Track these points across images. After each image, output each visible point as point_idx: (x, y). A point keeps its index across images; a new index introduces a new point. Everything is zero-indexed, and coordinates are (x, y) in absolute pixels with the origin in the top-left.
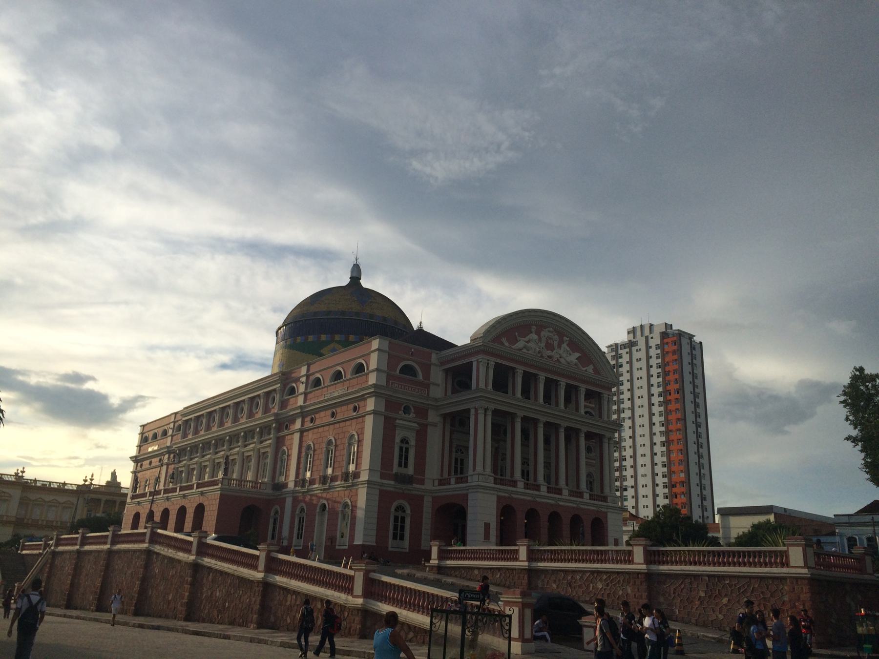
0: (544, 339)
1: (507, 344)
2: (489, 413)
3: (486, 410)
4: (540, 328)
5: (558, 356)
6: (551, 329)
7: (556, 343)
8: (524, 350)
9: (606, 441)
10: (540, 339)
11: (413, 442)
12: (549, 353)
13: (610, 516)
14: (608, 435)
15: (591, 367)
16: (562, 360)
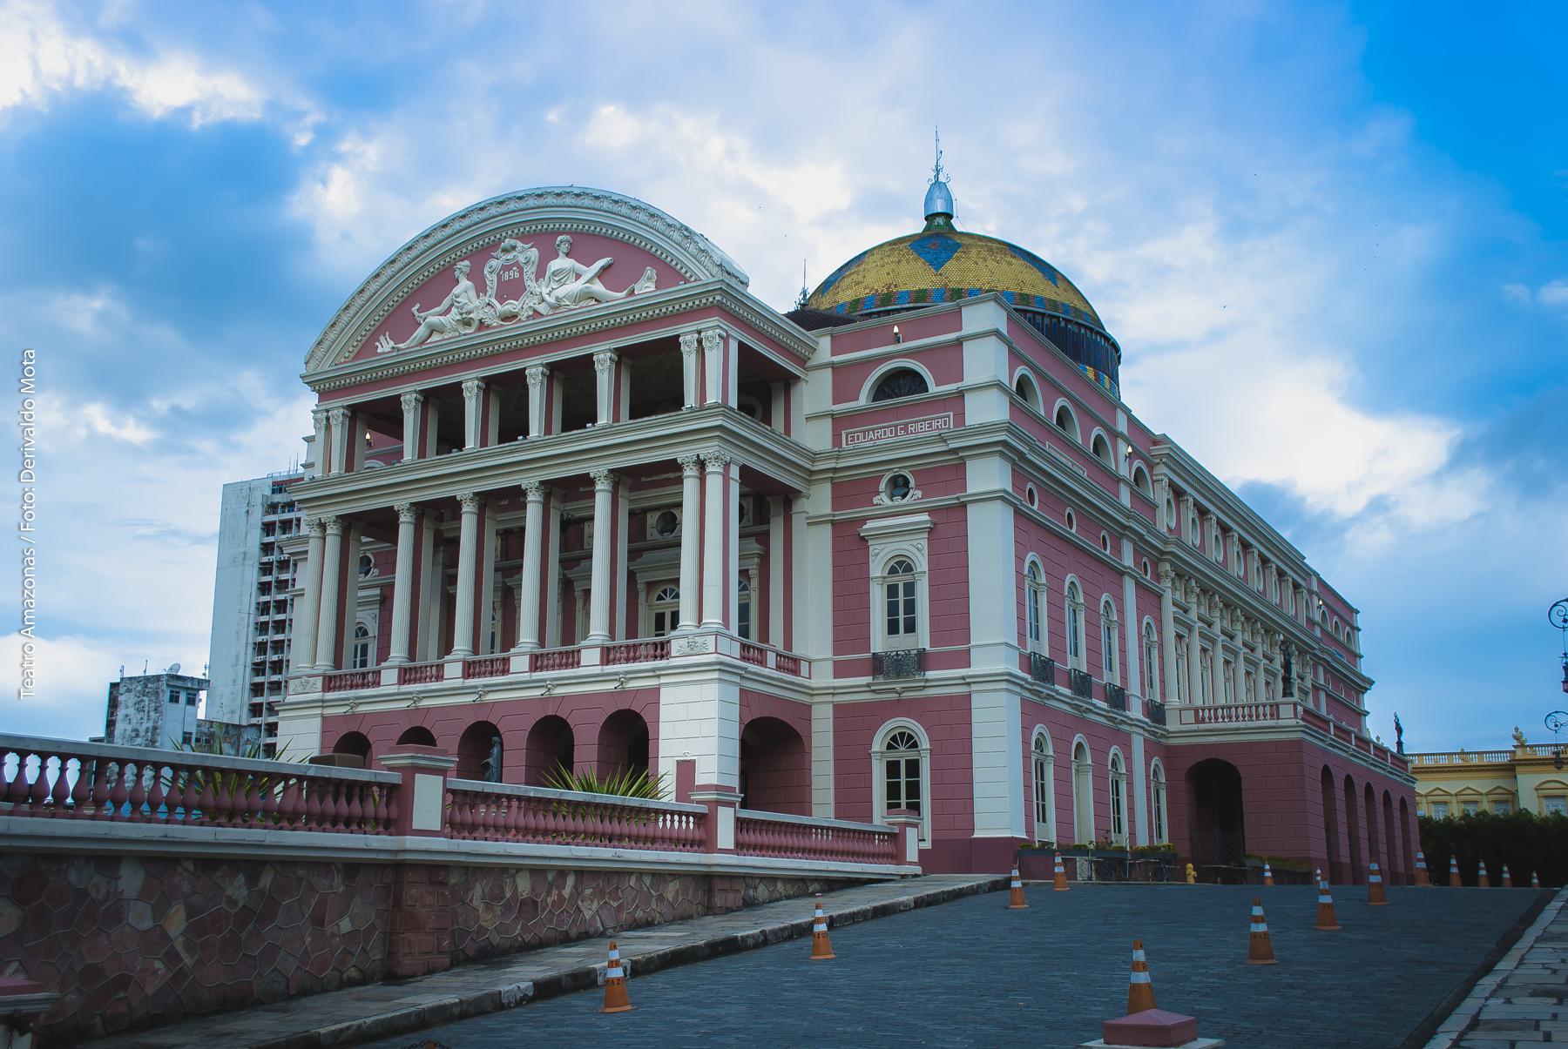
0: (491, 280)
1: (392, 344)
2: (332, 530)
3: (322, 526)
4: (480, 253)
5: (532, 302)
6: (508, 242)
7: (530, 271)
8: (435, 337)
9: (690, 472)
10: (481, 288)
11: (373, 630)
12: (512, 306)
13: (666, 696)
14: (683, 454)
15: (650, 271)
16: (542, 308)
